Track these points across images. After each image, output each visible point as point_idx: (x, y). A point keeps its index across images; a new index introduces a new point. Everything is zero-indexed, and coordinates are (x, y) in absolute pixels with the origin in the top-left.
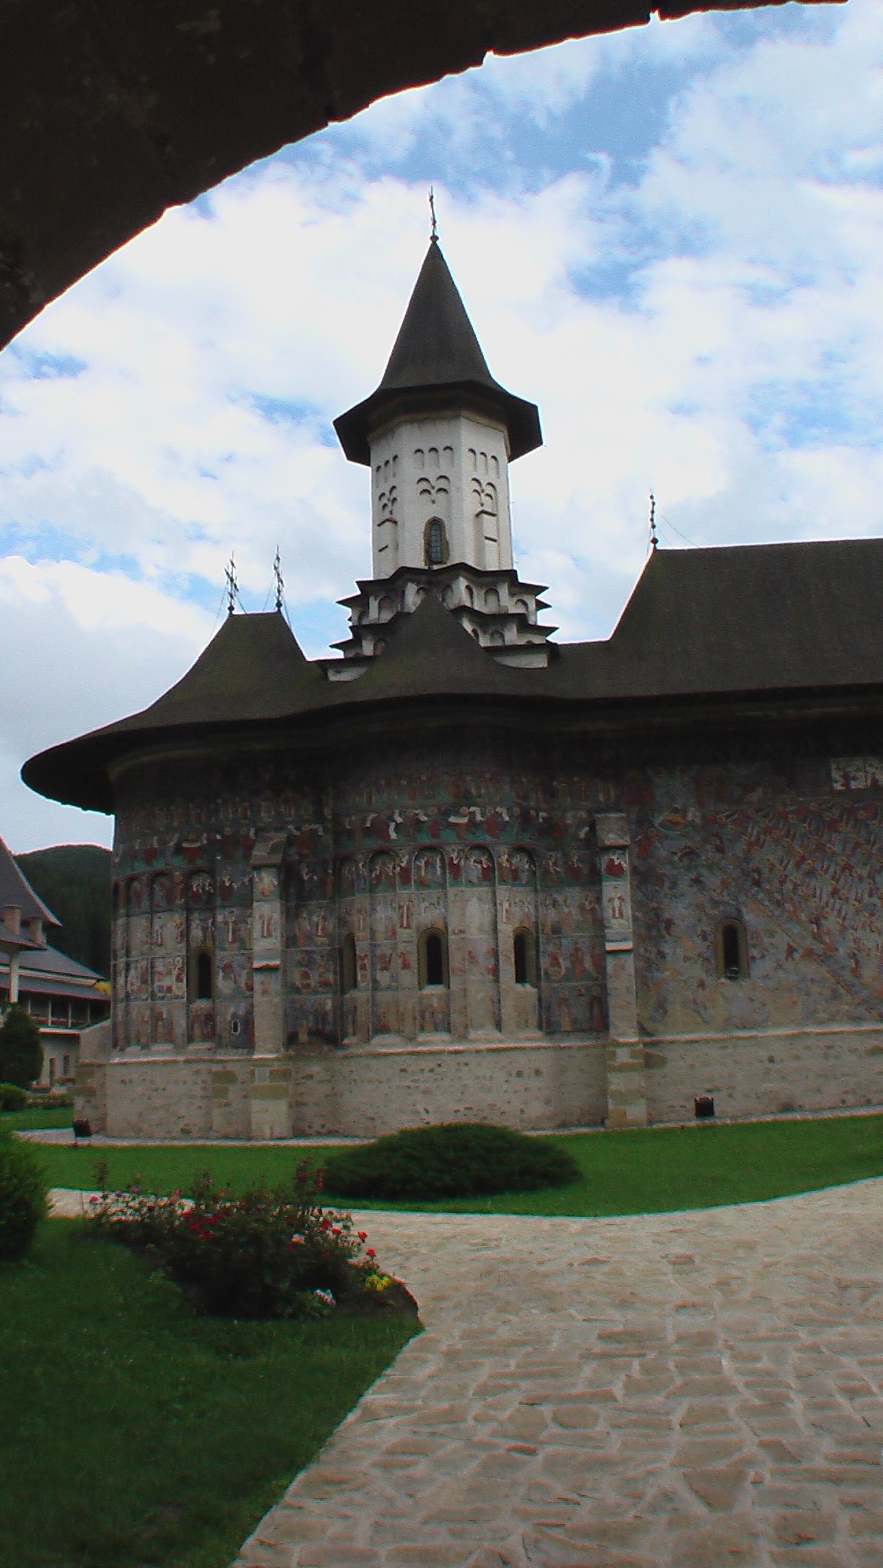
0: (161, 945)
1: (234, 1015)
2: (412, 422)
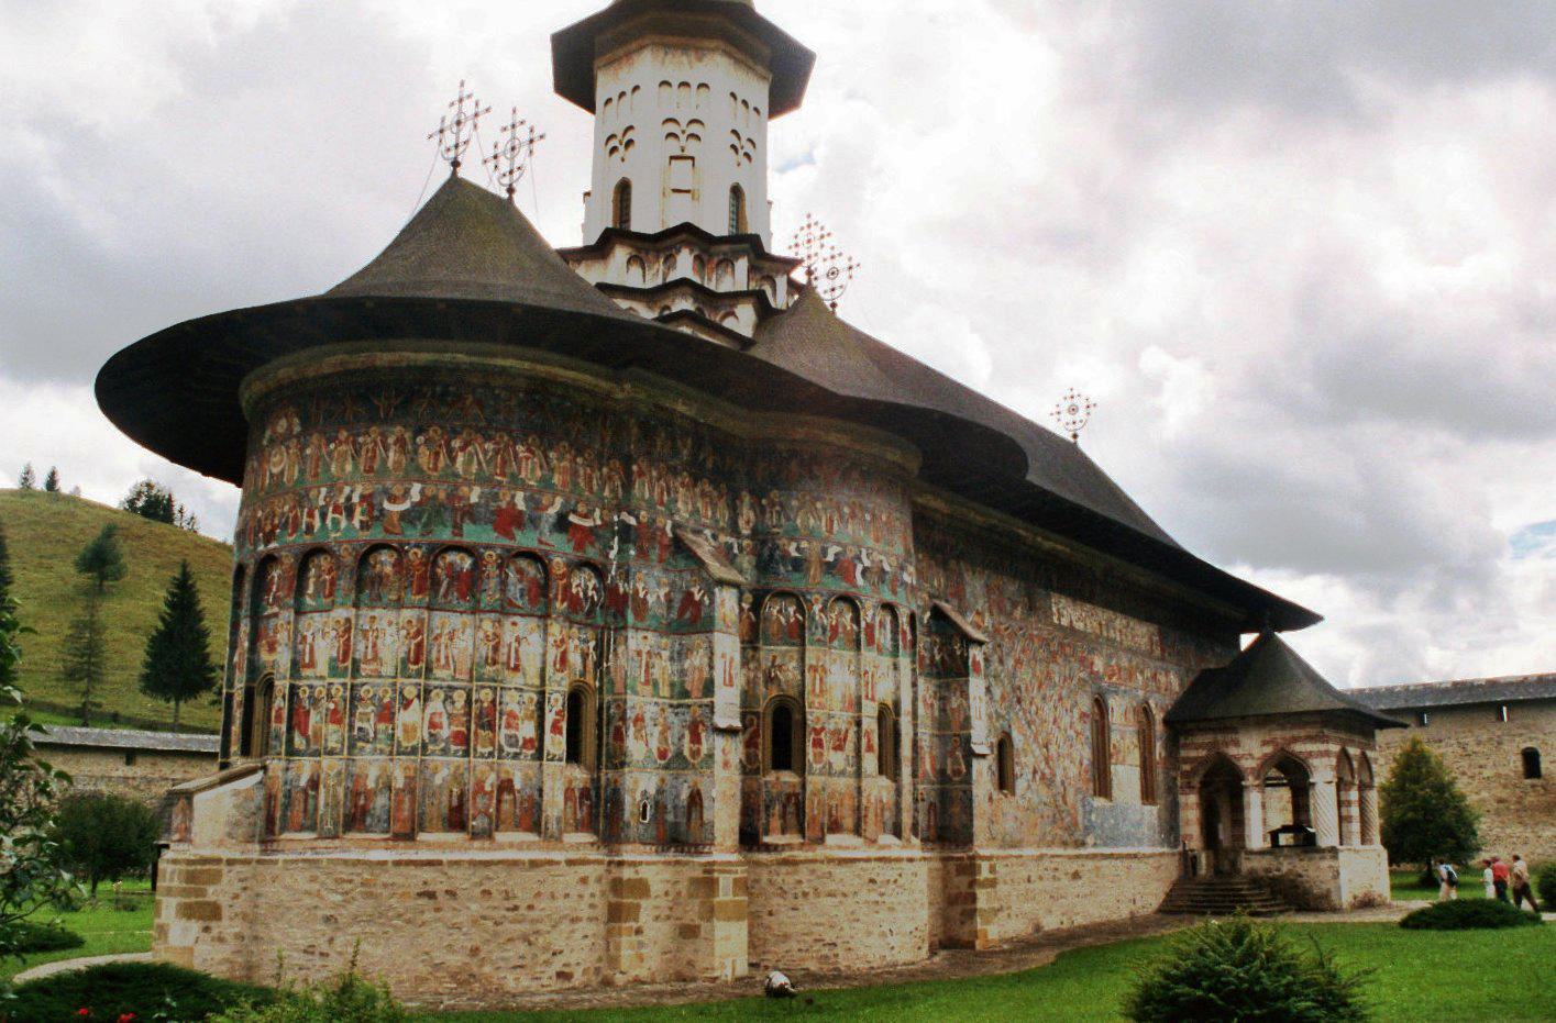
0: (516, 668)
1: (645, 793)
2: (727, 54)
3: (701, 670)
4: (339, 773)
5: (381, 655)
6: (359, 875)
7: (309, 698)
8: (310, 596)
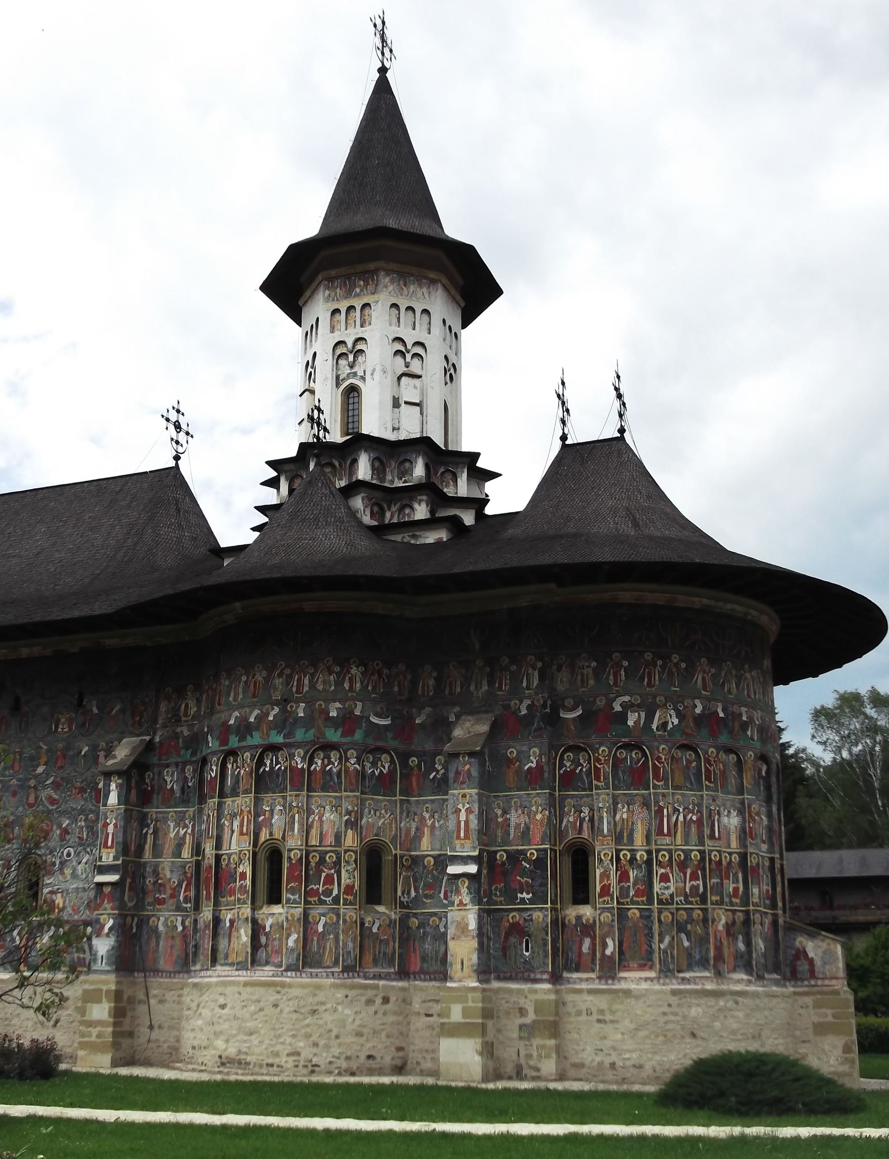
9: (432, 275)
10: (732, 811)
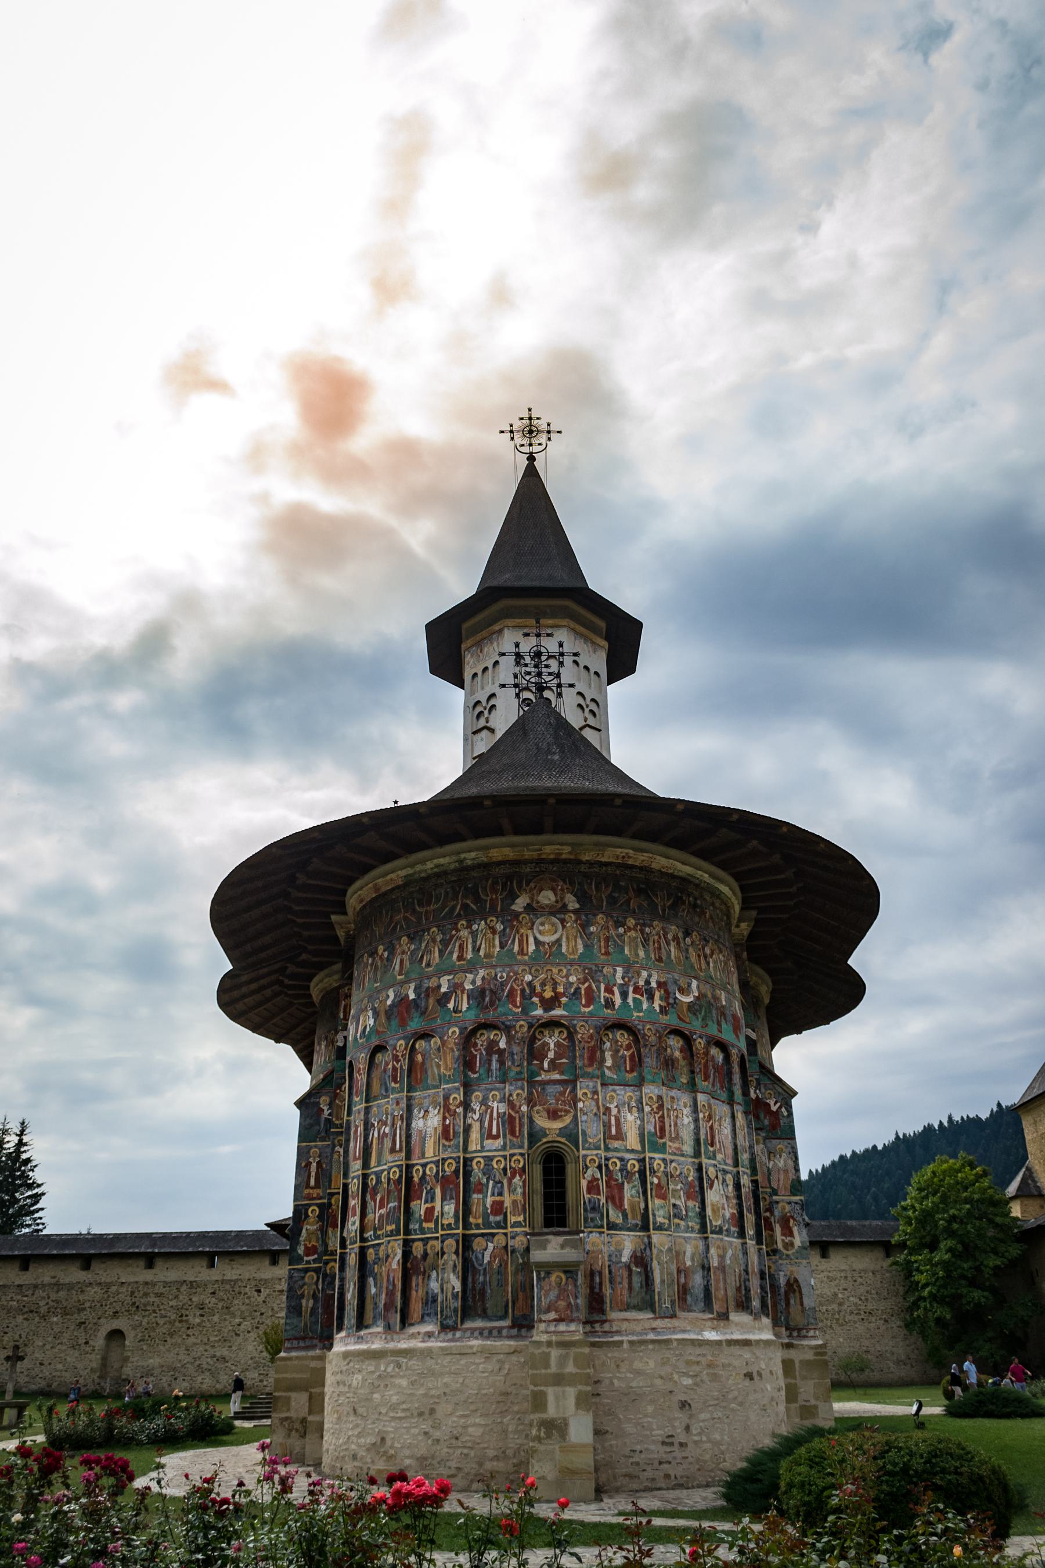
3: (786, 1171)
4: (670, 1250)
5: (681, 1134)
6: (704, 1355)
7: (621, 1170)
8: (609, 1068)
9: (496, 627)
10: (431, 1109)
